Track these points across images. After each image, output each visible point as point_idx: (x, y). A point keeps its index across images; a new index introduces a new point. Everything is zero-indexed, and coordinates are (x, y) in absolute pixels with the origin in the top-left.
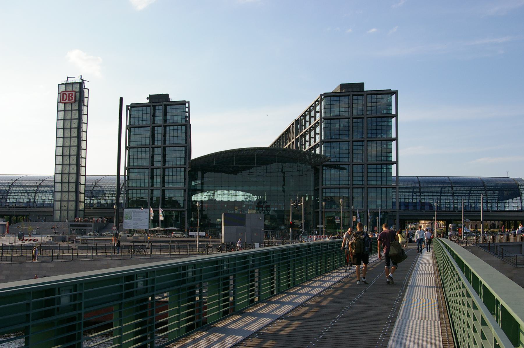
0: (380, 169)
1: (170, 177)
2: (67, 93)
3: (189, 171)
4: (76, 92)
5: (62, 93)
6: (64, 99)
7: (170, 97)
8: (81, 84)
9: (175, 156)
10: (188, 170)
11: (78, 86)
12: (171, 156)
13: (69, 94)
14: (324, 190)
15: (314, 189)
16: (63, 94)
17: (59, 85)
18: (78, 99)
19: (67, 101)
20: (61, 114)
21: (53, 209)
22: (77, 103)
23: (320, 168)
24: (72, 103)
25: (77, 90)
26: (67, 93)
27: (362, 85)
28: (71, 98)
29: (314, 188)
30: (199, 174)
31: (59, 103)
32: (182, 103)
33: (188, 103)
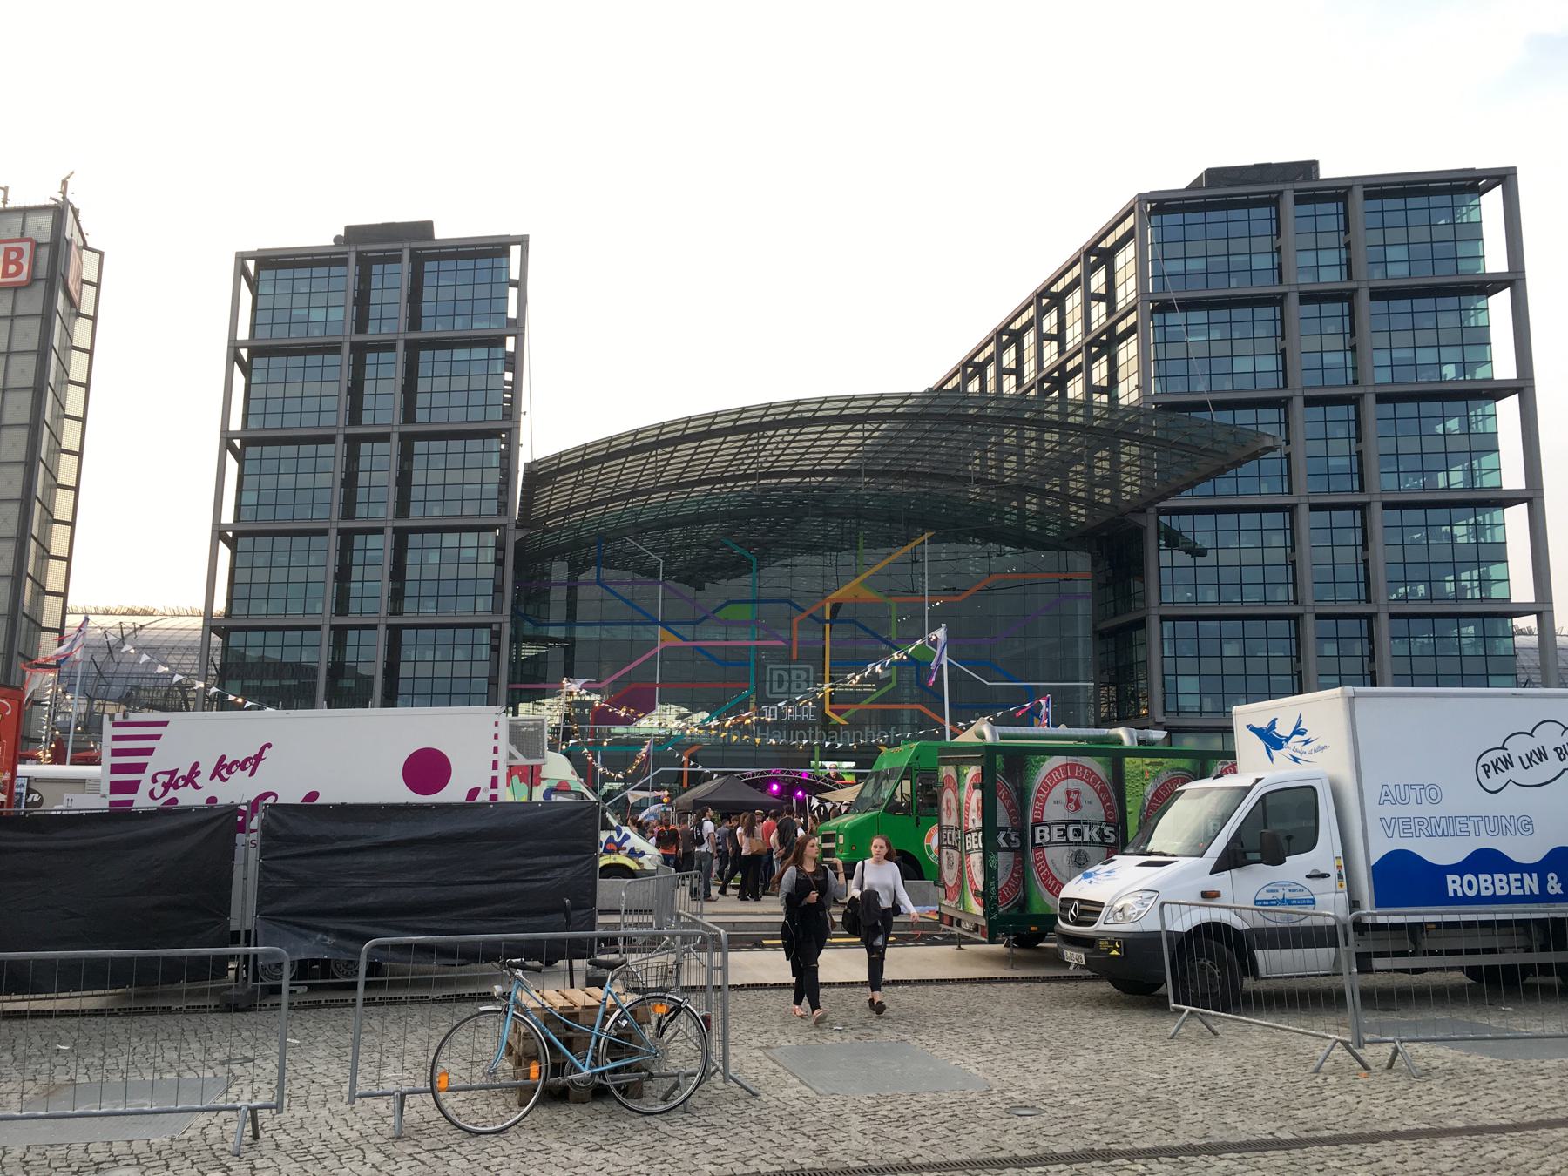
0: (1443, 529)
1: (429, 573)
3: (516, 543)
4: (37, 246)
8: (60, 212)
9: (454, 477)
10: (514, 536)
12: (435, 477)
14: (1168, 625)
15: (1094, 632)
18: (42, 272)
22: (40, 288)
23: (1149, 522)
24: (16, 288)
25: (45, 236)
27: (1313, 165)
28: (12, 268)
29: (1094, 626)
30: (560, 570)
32: (496, 249)
33: (523, 241)
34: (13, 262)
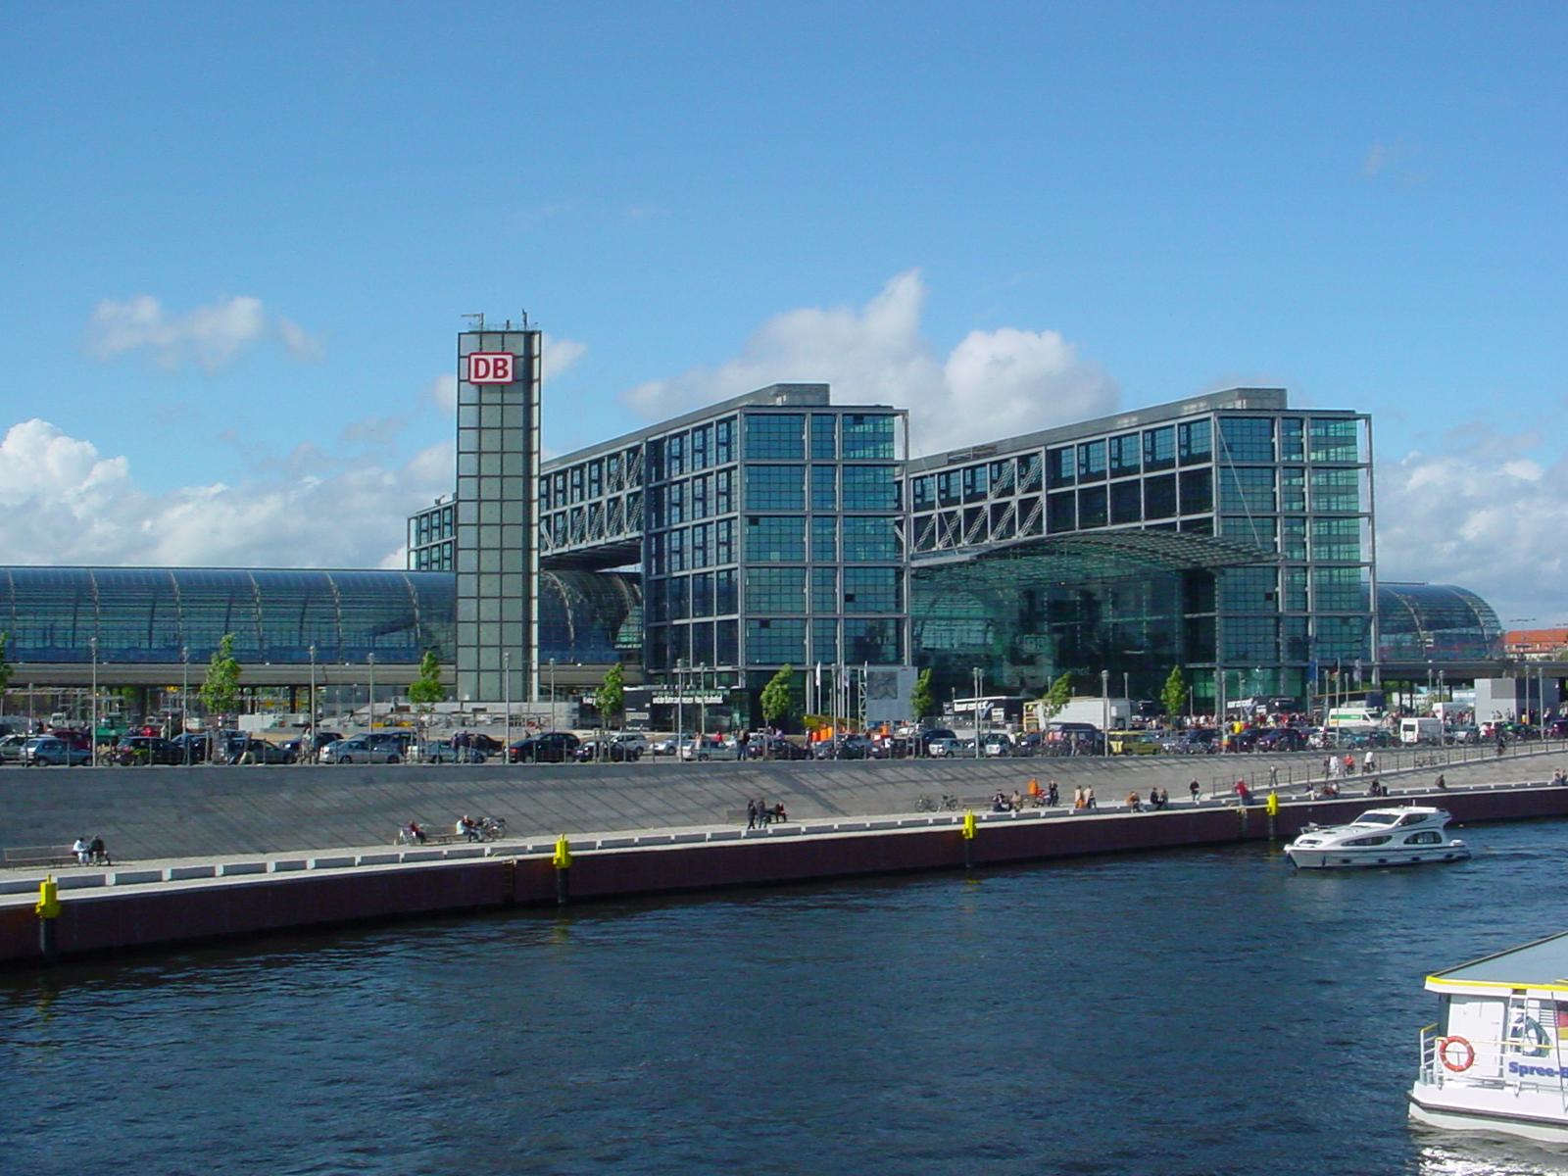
2: (490, 359)
4: (518, 357)
5: (473, 358)
6: (482, 372)
7: (832, 391)
11: (521, 339)
13: (496, 361)
16: (477, 361)
17: (459, 334)
19: (490, 378)
20: (469, 414)
21: (453, 667)
22: (521, 385)
25: (520, 350)
26: (490, 359)
31: (462, 384)
34: (500, 368)
